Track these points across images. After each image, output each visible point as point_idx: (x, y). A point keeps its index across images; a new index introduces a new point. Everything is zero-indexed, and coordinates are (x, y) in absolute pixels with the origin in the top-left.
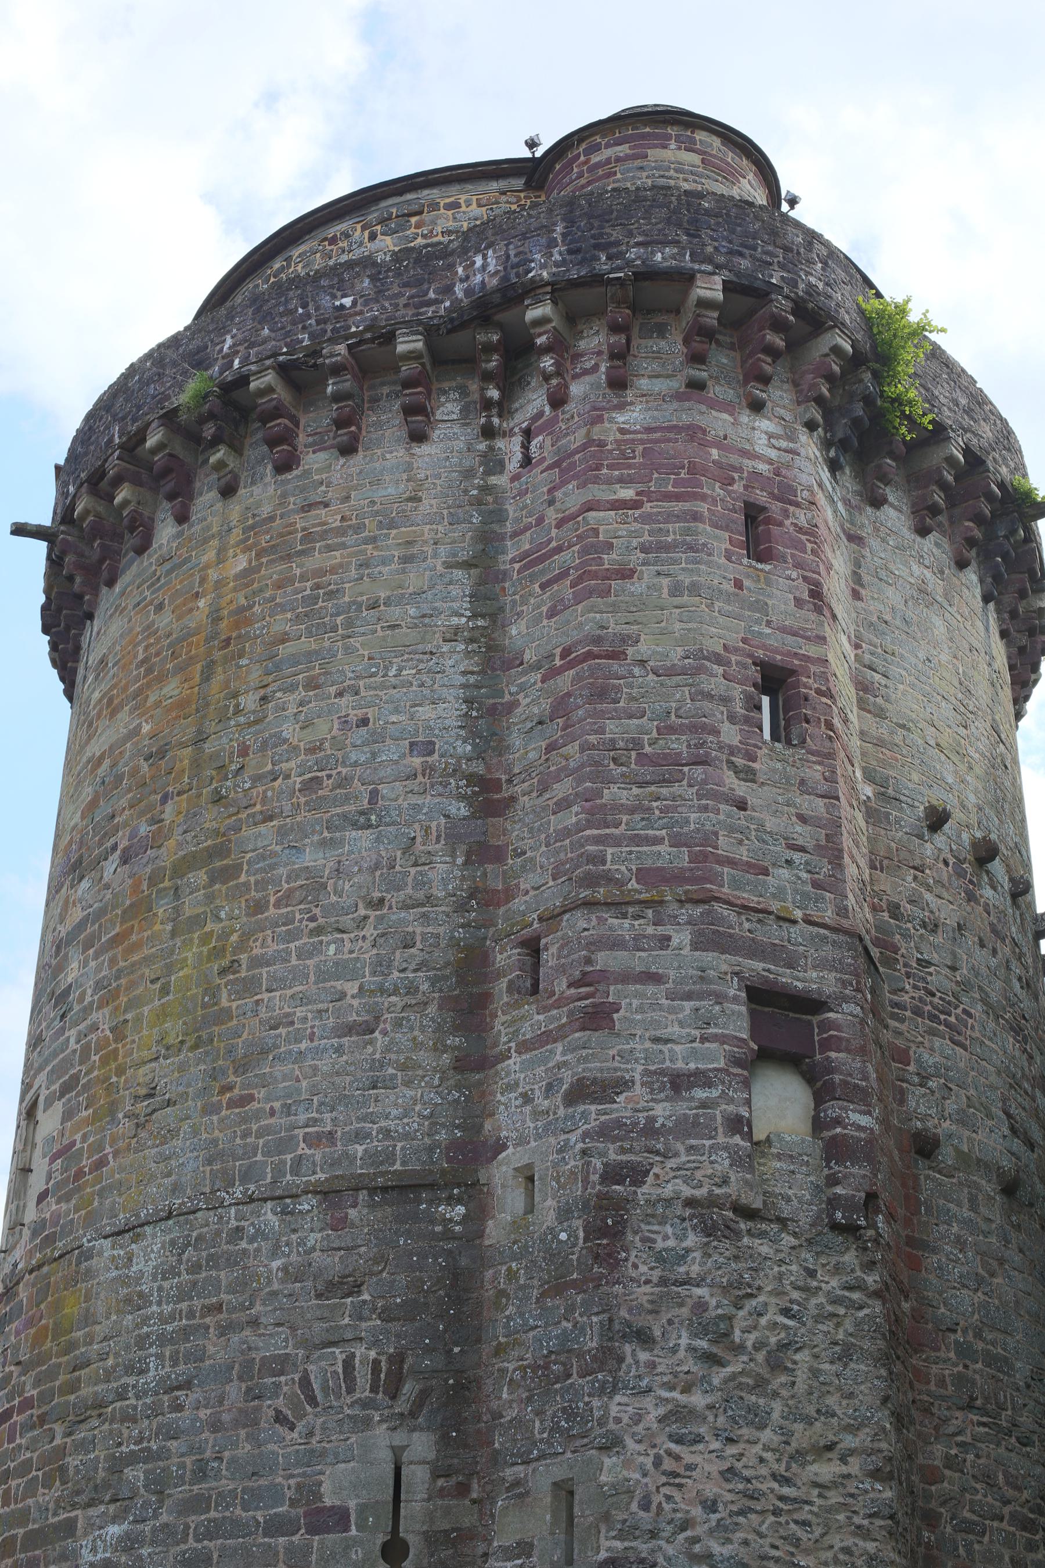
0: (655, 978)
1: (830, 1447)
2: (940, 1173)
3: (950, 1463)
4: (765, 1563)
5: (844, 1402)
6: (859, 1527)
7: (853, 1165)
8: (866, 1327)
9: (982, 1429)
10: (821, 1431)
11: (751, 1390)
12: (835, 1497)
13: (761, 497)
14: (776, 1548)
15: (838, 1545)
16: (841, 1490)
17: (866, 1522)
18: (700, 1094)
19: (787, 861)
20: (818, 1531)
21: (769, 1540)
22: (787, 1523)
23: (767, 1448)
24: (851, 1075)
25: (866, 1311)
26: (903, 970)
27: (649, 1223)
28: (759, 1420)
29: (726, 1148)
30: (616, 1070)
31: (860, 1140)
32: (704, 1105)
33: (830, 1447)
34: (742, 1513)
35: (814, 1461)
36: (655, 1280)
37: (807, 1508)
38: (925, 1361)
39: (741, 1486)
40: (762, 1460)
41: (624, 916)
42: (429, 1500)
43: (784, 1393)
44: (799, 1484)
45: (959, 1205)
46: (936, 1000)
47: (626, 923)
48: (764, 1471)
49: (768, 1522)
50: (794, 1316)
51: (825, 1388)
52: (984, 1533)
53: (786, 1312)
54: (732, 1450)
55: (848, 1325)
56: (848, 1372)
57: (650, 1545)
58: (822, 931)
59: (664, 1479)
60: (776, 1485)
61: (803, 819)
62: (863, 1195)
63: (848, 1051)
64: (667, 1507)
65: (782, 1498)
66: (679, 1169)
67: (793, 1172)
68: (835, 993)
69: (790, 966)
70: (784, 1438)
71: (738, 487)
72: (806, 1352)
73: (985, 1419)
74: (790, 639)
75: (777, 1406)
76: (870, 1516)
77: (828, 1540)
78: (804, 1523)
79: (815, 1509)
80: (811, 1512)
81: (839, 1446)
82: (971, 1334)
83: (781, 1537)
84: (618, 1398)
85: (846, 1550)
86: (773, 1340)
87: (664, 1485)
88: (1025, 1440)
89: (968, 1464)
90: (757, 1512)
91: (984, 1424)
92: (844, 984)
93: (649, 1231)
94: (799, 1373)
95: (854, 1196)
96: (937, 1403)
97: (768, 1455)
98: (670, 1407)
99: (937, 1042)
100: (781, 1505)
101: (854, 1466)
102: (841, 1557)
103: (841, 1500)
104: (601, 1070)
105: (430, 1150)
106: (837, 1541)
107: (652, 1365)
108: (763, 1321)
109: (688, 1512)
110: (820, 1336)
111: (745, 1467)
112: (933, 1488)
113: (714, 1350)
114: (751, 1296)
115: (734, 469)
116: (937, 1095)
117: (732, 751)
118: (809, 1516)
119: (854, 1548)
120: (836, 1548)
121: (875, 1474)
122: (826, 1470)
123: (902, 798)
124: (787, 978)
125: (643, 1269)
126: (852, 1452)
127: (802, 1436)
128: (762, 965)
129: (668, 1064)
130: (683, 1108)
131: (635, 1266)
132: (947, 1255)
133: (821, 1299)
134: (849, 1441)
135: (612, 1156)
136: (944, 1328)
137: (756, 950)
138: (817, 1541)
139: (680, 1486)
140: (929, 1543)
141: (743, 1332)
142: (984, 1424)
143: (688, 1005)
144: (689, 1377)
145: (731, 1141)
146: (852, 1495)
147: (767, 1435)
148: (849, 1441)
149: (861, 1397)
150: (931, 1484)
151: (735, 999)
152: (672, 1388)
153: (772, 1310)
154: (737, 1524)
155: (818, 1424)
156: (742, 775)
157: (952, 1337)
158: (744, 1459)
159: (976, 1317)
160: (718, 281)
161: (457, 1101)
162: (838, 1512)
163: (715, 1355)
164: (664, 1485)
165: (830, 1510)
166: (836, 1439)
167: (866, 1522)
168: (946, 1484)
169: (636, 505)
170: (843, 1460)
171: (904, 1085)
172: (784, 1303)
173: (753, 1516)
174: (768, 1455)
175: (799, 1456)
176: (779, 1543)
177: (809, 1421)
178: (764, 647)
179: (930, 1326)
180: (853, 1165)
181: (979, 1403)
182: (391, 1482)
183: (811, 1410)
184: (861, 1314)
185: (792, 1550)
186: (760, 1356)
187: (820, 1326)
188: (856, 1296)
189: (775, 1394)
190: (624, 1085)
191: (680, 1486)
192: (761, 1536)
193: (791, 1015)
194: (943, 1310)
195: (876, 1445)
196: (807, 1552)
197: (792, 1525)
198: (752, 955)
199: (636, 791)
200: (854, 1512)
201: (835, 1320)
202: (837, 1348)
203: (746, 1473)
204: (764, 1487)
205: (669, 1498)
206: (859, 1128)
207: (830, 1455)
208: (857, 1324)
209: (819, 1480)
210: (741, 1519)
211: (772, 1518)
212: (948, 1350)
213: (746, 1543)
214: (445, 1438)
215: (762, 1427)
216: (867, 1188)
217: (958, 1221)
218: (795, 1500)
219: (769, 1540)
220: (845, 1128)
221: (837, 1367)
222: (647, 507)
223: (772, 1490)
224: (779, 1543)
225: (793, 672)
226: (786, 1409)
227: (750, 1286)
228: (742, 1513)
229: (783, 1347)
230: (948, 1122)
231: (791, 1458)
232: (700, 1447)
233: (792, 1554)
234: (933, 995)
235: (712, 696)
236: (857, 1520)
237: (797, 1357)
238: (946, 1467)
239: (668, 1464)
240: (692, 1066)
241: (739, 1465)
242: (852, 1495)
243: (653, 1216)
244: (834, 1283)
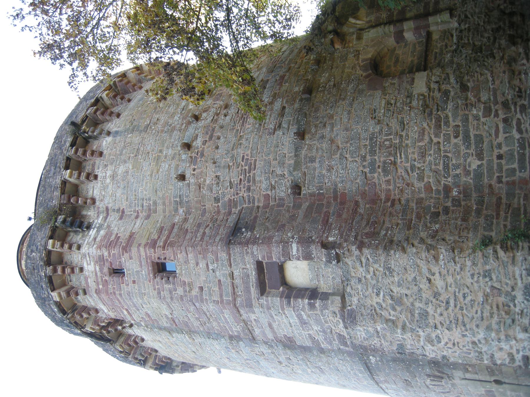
0: (270, 325)
1: (429, 280)
2: (305, 180)
3: (421, 178)
4: (484, 318)
5: (409, 272)
6: (461, 269)
7: (313, 254)
8: (376, 258)
9: (403, 156)
10: (424, 285)
11: (413, 315)
12: (450, 280)
13: (106, 270)
14: (477, 311)
15: (470, 280)
16: (446, 277)
17: (459, 265)
18: (305, 317)
19: (213, 272)
20: (466, 290)
21: (474, 315)
22: (465, 304)
23: (435, 312)
24: (279, 253)
25: (369, 257)
26: (236, 196)
27: (358, 338)
28: (424, 315)
29: (322, 311)
30: (307, 338)
31: (302, 250)
32: (309, 316)
33: (429, 280)
34: (465, 326)
35: (437, 287)
36: (379, 339)
37: (457, 294)
38: (381, 192)
39: (454, 326)
40: (441, 315)
41: (253, 330)
42: (477, 373)
43: (411, 300)
44: (447, 297)
45: (315, 169)
46: (242, 178)
47: (256, 330)
48: (445, 314)
49: (467, 313)
50: (379, 292)
51: (405, 281)
52: (448, 157)
53: (378, 295)
54: (439, 326)
55: (376, 266)
56: (396, 269)
57: (484, 354)
58: (232, 261)
59: (456, 347)
60: (451, 309)
61: (197, 264)
62: (323, 250)
63: (271, 253)
64: (467, 348)
65: (455, 306)
66: (335, 326)
67: (323, 275)
68: (252, 257)
69: (248, 276)
70: (430, 303)
71: (107, 278)
72: (392, 287)
73: (398, 155)
74: (143, 263)
75: (417, 304)
76: (455, 263)
77: (469, 284)
78: (464, 297)
79: (457, 290)
80: (459, 293)
81: (428, 276)
82: (364, 163)
83: (472, 308)
84: (428, 354)
85: (473, 275)
86: (391, 302)
87: (459, 347)
88: (402, 125)
89: (419, 166)
90: (463, 319)
91: (401, 155)
92: (247, 253)
93: (361, 338)
94: (401, 292)
95: (325, 254)
96: (398, 185)
97: (439, 311)
98: (427, 343)
99: (257, 179)
100: (458, 307)
101: (435, 269)
102: (475, 279)
103: (451, 277)
104: (308, 342)
105: (354, 362)
106: (469, 281)
107: (411, 345)
108: (384, 305)
109: (468, 342)
110: (384, 280)
111: (445, 322)
112: (434, 188)
113: (400, 327)
114: (375, 310)
115: (102, 280)
116: (277, 180)
117: (185, 291)
118: (461, 294)
119: (471, 272)
120: (472, 281)
121: (436, 258)
122: (439, 283)
123: (179, 194)
124: (253, 275)
125: (375, 342)
126: (429, 270)
127: (427, 294)
128: (252, 288)
129: (298, 324)
130: (312, 322)
131: (375, 343)
132: (336, 177)
133: (369, 277)
134: (425, 270)
135: (337, 342)
136: (365, 180)
137: (247, 290)
138: (471, 292)
139: (458, 343)
140: (458, 192)
141: (390, 315)
142: (401, 155)
143: (275, 317)
144: (413, 336)
145: (318, 308)
146: (448, 271)
147: (430, 309)
148: (425, 270)
149: (405, 264)
150: (432, 190)
151: (267, 301)
152: (420, 340)
153: (378, 300)
154: (470, 329)
155: (421, 286)
156: (192, 286)
157: (368, 175)
158: (442, 321)
159: (357, 159)
160: (52, 294)
161: (335, 354)
162: (456, 279)
163: (402, 326)
164: (459, 347)
165: (456, 283)
166: (426, 278)
167: (459, 265)
168: (431, 180)
169: (127, 310)
170: (433, 274)
171: (277, 198)
172: (374, 295)
173: (466, 320)
174: (439, 311)
175: (436, 295)
176: (474, 310)
177: (420, 290)
178: (149, 274)
179: (367, 188)
180: (313, 254)
181: (392, 159)
182: (473, 382)
183: (416, 288)
184: (371, 260)
185: (476, 303)
186: (399, 309)
187: (380, 280)
188: (364, 261)
189: (412, 304)
190: (310, 335)
191: (458, 343)
192: (473, 318)
193: (265, 271)
194: (358, 181)
195: (424, 258)
196: (476, 296)
197: (466, 302)
198: (249, 292)
199: (211, 320)
200: (455, 270)
201: (376, 272)
202: (387, 273)
203: (448, 323)
204: (453, 315)
205: (464, 346)
206: (298, 250)
207: (433, 281)
208: (376, 262)
209: (444, 287)
210: (468, 326)
211: (465, 311)
212: (374, 178)
213: (477, 326)
214: (454, 369)
215: (427, 313)
216: (320, 248)
217: (321, 170)
218: (455, 300)
219: (474, 315)
220: (300, 256)
221: (395, 274)
222: (126, 307)
223: (453, 310)
224: (474, 310)
225: (153, 262)
226: (418, 301)
227: (372, 310)
228: (465, 326)
229: (392, 298)
230: (285, 173)
231: (437, 299)
232: (441, 336)
233: (478, 304)
234: (241, 179)
235: (171, 297)
236: (458, 269)
237: (395, 291)
238: (423, 181)
239: (450, 345)
240: (296, 318)
241: (445, 325)
242: (448, 271)
243: (355, 337)
244: (361, 269)
